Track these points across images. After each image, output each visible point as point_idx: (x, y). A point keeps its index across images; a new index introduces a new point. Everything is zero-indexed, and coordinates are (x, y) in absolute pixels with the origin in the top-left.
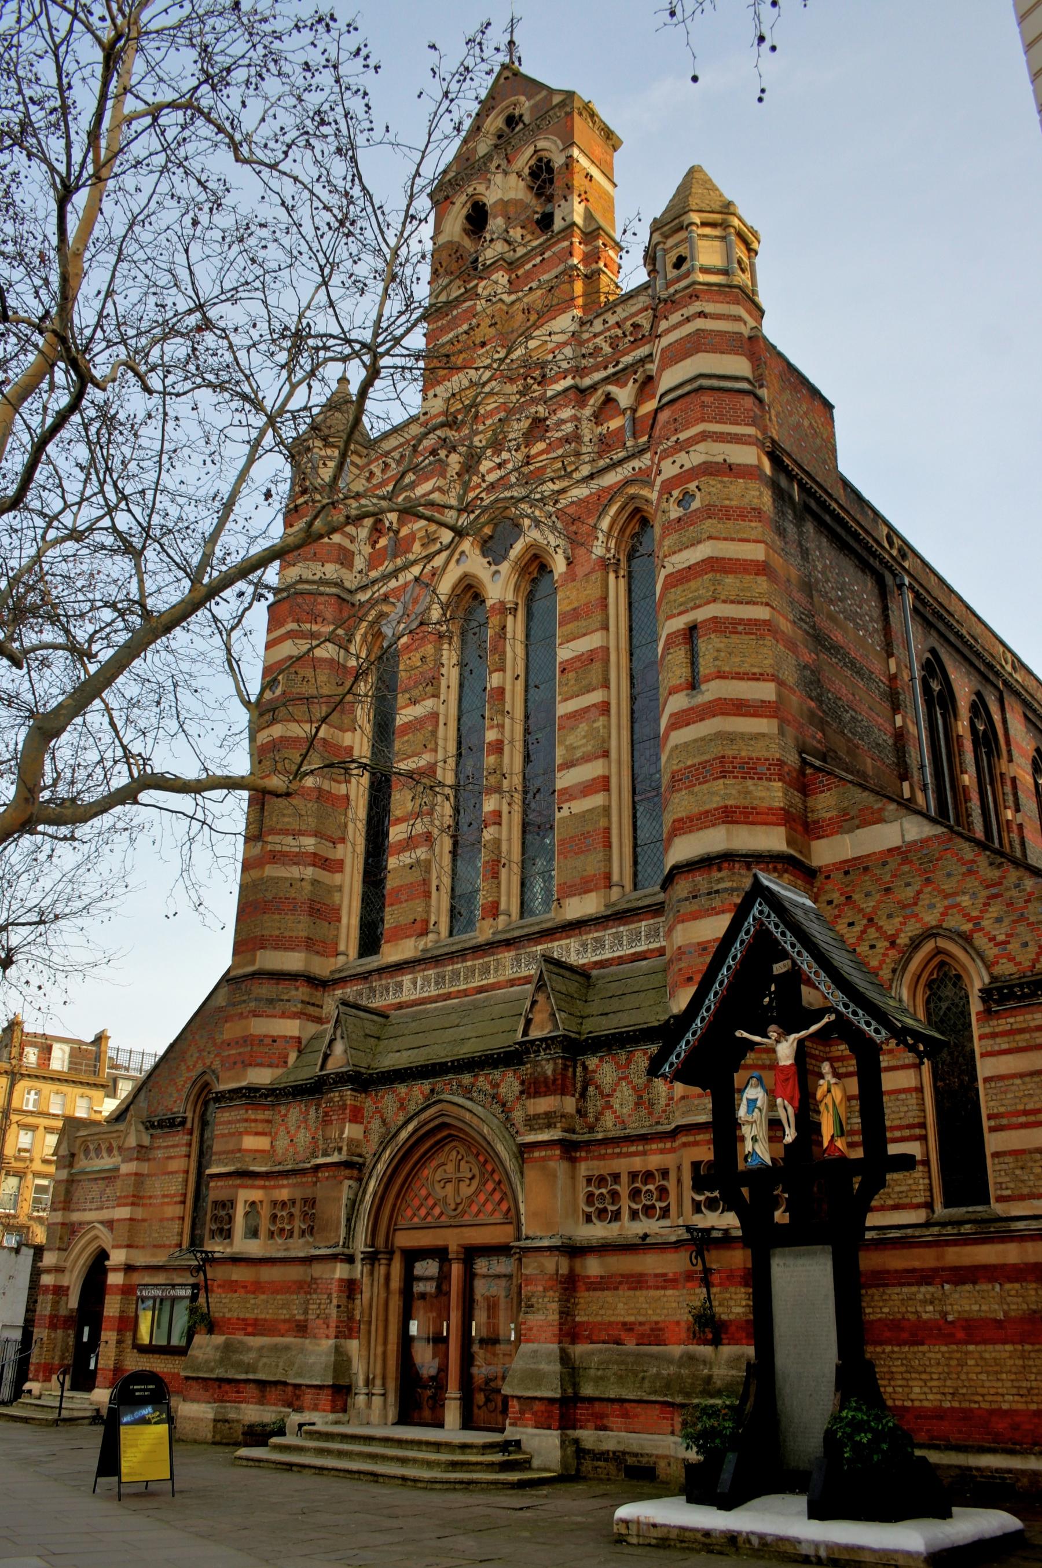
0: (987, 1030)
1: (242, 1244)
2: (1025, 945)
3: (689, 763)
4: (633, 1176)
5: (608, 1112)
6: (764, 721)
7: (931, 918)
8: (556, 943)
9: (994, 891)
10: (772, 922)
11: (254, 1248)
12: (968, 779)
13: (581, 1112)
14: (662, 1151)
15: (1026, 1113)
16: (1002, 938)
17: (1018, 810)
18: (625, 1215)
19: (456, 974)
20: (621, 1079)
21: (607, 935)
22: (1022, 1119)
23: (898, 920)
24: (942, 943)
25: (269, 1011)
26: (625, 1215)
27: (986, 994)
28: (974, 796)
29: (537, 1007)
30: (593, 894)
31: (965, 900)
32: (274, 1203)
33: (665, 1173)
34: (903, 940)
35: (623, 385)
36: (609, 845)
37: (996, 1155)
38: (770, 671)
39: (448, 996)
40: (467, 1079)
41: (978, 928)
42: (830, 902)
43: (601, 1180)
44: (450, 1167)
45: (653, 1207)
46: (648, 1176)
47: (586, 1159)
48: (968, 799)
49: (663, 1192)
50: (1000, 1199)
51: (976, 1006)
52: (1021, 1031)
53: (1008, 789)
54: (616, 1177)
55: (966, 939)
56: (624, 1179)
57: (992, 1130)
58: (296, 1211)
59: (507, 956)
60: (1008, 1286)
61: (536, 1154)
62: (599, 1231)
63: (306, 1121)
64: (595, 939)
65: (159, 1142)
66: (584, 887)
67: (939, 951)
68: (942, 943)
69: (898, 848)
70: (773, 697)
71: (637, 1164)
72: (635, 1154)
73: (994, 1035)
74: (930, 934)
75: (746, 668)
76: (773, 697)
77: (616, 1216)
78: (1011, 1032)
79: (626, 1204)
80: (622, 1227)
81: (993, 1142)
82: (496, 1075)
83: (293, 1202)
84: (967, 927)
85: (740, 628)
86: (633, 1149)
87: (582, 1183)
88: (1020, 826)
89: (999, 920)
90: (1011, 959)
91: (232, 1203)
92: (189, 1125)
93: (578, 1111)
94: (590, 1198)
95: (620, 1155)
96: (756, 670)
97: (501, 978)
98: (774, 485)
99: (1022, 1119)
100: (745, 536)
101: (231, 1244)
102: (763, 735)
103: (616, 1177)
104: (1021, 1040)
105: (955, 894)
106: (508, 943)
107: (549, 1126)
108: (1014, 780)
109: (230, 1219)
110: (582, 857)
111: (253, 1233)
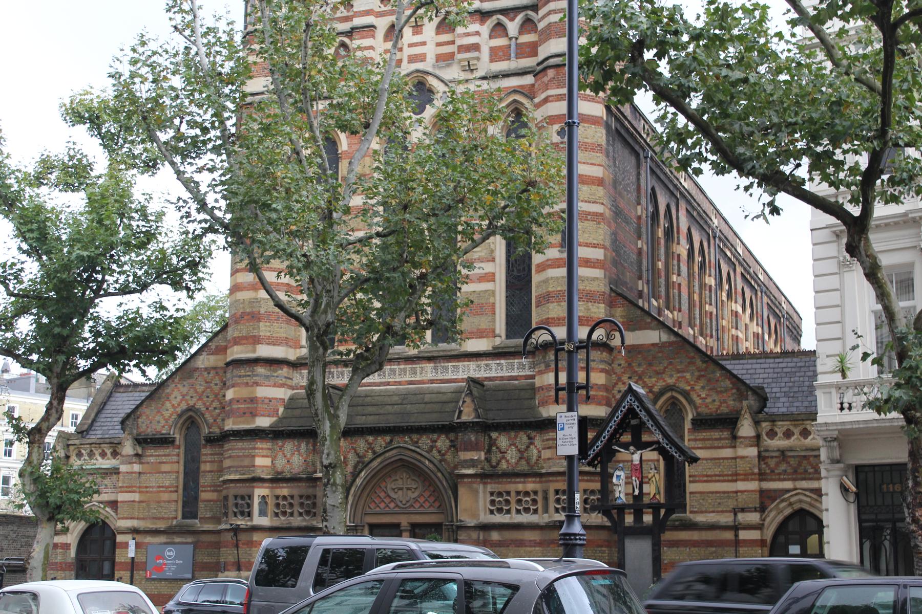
0: (693, 437)
1: (259, 520)
2: (714, 401)
3: (559, 289)
4: (518, 493)
5: (503, 461)
6: (597, 271)
7: (671, 381)
8: (461, 364)
9: (703, 373)
10: (636, 405)
11: (265, 521)
12: (660, 265)
13: (488, 460)
14: (534, 482)
15: (707, 476)
16: (703, 396)
17: (679, 275)
18: (513, 511)
19: (394, 371)
20: (511, 445)
21: (493, 363)
22: (705, 479)
23: (654, 379)
24: (675, 394)
25: (267, 383)
26: (513, 511)
27: (694, 422)
28: (663, 274)
29: (466, 404)
30: (485, 340)
31: (688, 376)
32: (277, 497)
33: (535, 493)
34: (656, 389)
35: (512, 20)
36: (494, 313)
37: (691, 493)
38: (602, 242)
39: (388, 384)
40: (415, 437)
41: (693, 389)
42: (620, 365)
43: (500, 494)
44: (400, 482)
45: (529, 508)
46: (527, 494)
47: (491, 483)
48: (659, 277)
49: (535, 502)
50: (691, 512)
51: (688, 425)
52: (708, 440)
53: (675, 262)
54: (508, 493)
55: (686, 395)
56: (513, 494)
57: (690, 482)
58: (296, 502)
59: (429, 366)
60: (692, 549)
61: (466, 480)
62: (498, 518)
63: (299, 451)
64: (487, 365)
65: (149, 452)
66: (480, 334)
67: (673, 397)
68: (675, 394)
69: (657, 344)
70: (602, 258)
71: (520, 487)
72: (519, 482)
73: (696, 440)
74: (670, 388)
75: (590, 240)
76: (602, 258)
77: (508, 512)
78: (703, 440)
79: (514, 506)
80: (511, 518)
81: (691, 487)
82: (435, 436)
83: (292, 497)
84: (688, 388)
85: (589, 217)
86: (518, 480)
87: (489, 495)
88: (679, 285)
89: (703, 388)
90: (707, 406)
91: (250, 497)
92: (177, 443)
93: (486, 459)
94: (493, 502)
95: (510, 482)
96: (595, 242)
97: (425, 378)
98: (608, 127)
99: (705, 479)
100: (594, 162)
101: (252, 520)
102: (597, 278)
103: (508, 493)
104: (708, 443)
105: (683, 372)
106: (430, 359)
107: (473, 466)
108: (679, 256)
109: (249, 506)
110: (478, 317)
111: (263, 513)
